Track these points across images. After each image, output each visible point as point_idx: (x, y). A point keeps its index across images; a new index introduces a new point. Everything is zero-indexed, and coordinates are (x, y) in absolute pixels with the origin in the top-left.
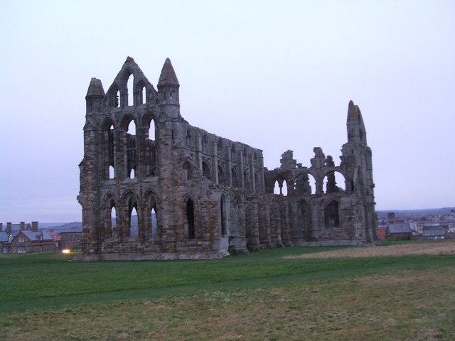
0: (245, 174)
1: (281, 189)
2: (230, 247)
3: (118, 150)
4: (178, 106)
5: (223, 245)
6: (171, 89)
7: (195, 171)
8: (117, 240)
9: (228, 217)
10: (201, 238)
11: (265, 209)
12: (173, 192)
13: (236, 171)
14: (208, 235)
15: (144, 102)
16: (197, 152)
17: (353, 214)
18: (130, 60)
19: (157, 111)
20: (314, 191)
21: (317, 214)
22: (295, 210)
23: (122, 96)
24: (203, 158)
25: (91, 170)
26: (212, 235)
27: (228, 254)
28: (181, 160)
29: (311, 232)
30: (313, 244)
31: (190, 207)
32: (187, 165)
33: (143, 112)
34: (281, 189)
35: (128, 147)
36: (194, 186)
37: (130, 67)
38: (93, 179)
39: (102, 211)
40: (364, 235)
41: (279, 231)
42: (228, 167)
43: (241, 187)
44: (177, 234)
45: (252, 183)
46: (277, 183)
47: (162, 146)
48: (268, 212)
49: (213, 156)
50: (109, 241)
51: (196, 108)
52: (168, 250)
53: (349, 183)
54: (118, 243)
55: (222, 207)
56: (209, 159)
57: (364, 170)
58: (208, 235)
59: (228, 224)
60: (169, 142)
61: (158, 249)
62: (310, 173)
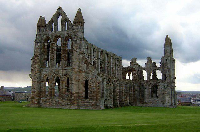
0: (113, 68)
1: (129, 77)
2: (105, 104)
3: (52, 53)
5: (102, 103)
6: (81, 24)
7: (90, 66)
8: (48, 98)
10: (91, 99)
11: (122, 87)
12: (79, 75)
13: (109, 66)
14: (95, 97)
15: (66, 29)
16: (91, 56)
17: (165, 92)
18: (60, 8)
19: (73, 34)
20: (145, 79)
21: (147, 91)
22: (136, 88)
23: (55, 26)
24: (94, 59)
27: (104, 108)
28: (83, 59)
29: (144, 99)
31: (86, 83)
32: (87, 62)
33: (66, 35)
34: (129, 77)
35: (57, 52)
36: (90, 73)
37: (60, 12)
38: (38, 66)
39: (42, 83)
40: (170, 102)
41: (129, 98)
42: (104, 64)
43: (111, 75)
44: (79, 96)
45: (116, 73)
46: (127, 74)
47: (74, 52)
48: (124, 88)
49: (98, 59)
50: (44, 98)
52: (74, 104)
53: (164, 76)
54: (49, 99)
55: (102, 85)
56: (96, 60)
57: (172, 70)
58: (95, 97)
59: (104, 93)
61: (69, 103)
62: (144, 70)
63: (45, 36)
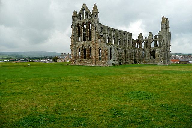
0: (124, 40)
2: (113, 63)
4: (98, 19)
6: (96, 14)
9: (113, 54)
16: (105, 34)
19: (91, 21)
25: (74, 39)
26: (106, 59)
27: (112, 65)
30: (146, 63)
33: (88, 21)
40: (163, 61)
42: (117, 38)
46: (136, 44)
48: (129, 53)
50: (78, 60)
51: (104, 20)
60: (94, 30)
63: (77, 23)
